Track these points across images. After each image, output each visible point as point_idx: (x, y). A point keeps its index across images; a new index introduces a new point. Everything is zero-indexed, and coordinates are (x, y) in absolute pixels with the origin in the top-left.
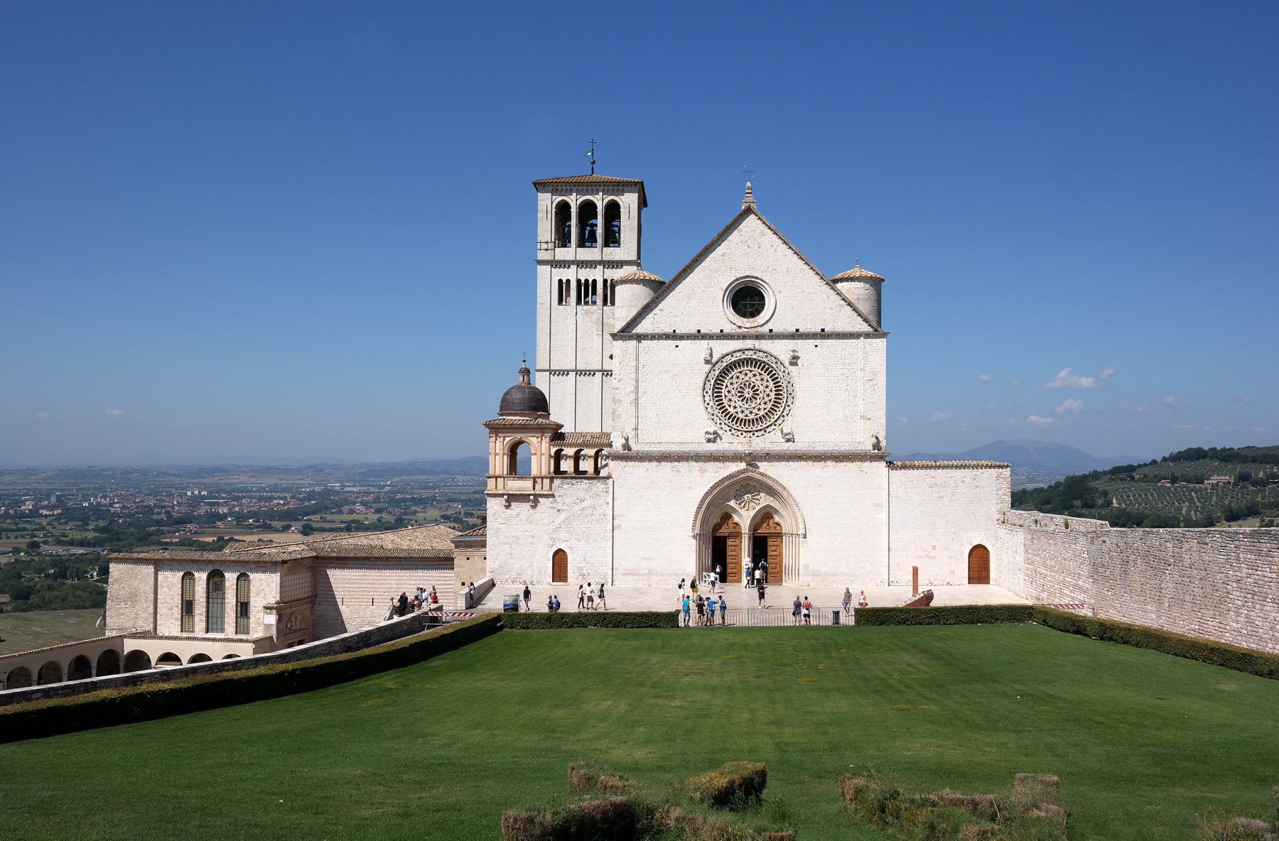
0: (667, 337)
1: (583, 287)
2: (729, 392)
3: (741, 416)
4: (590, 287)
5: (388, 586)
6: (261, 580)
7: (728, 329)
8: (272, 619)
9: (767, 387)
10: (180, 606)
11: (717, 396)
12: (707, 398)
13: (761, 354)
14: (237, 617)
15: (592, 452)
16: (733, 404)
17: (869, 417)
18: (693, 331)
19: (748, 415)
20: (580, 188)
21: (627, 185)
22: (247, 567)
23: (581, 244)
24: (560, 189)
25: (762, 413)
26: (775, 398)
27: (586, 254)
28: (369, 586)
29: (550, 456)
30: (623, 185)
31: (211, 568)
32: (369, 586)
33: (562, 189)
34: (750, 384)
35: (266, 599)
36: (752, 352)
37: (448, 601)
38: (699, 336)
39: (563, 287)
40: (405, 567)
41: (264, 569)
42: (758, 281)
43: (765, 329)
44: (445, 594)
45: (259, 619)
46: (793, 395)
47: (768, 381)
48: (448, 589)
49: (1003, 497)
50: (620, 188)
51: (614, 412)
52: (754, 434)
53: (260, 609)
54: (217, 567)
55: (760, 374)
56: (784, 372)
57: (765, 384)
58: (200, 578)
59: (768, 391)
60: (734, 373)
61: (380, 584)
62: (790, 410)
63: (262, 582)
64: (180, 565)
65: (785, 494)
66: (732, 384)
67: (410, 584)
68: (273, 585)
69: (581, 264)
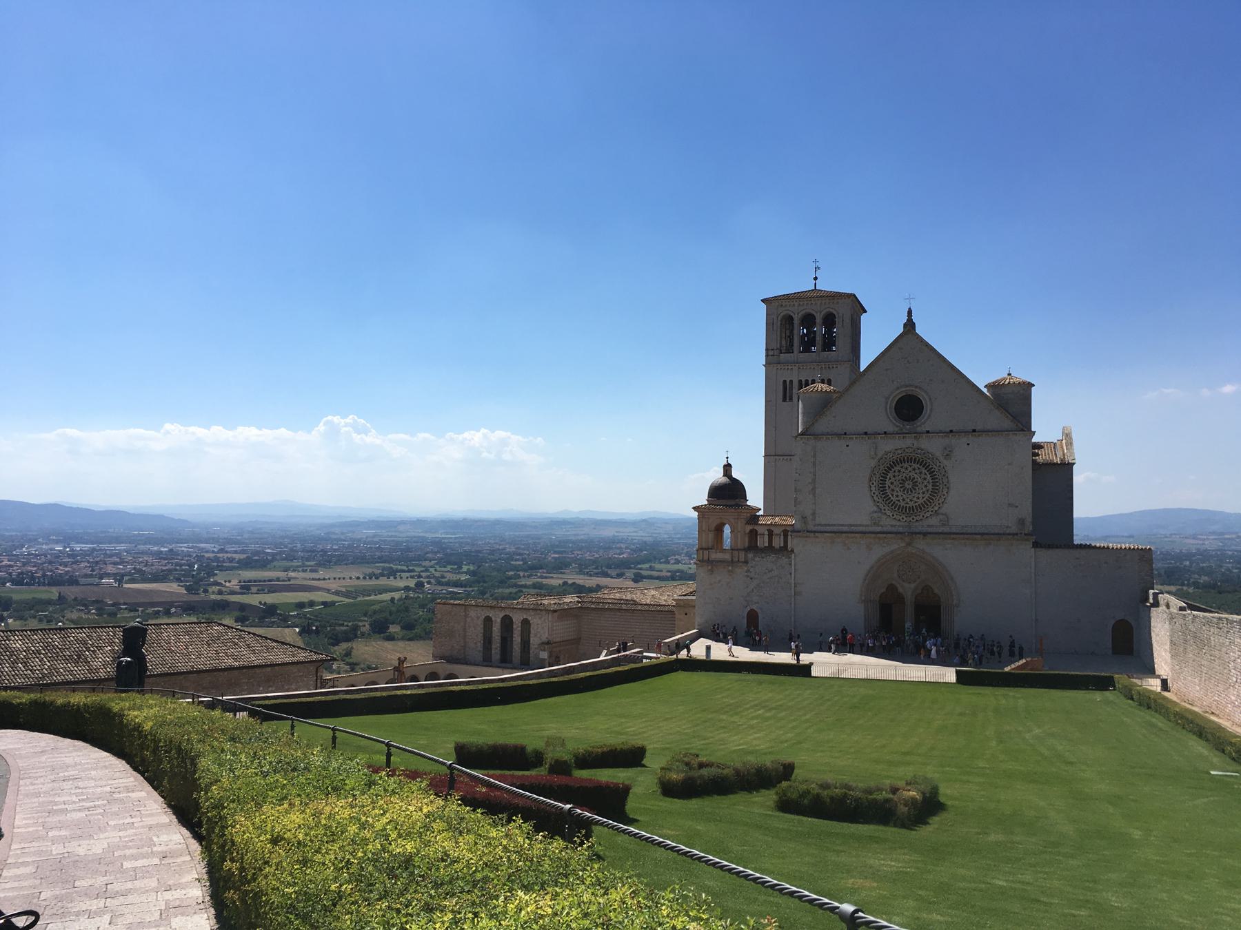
0: (838, 435)
2: (892, 483)
3: (902, 504)
7: (890, 429)
8: (544, 655)
9: (925, 479)
10: (482, 642)
11: (882, 488)
12: (873, 489)
13: (919, 451)
16: (895, 493)
17: (1017, 505)
19: (910, 503)
20: (801, 303)
24: (784, 304)
25: (921, 501)
26: (932, 489)
29: (745, 532)
30: (838, 299)
31: (502, 615)
32: (619, 632)
34: (910, 477)
42: (917, 390)
43: (925, 430)
46: (948, 485)
47: (925, 474)
49: (1146, 577)
50: (835, 301)
51: (796, 499)
52: (913, 519)
53: (536, 646)
54: (508, 614)
55: (919, 469)
56: (940, 466)
57: (923, 476)
58: (496, 620)
59: (926, 482)
62: (945, 499)
66: (894, 476)
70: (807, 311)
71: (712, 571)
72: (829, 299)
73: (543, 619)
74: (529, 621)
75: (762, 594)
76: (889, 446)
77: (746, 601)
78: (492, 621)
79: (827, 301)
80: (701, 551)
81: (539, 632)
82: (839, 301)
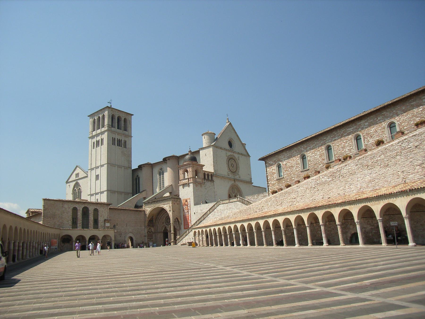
1: (118, 141)
5: (121, 219)
7: (229, 149)
10: (71, 220)
22: (97, 206)
23: (118, 128)
24: (113, 111)
25: (235, 170)
27: (119, 131)
31: (83, 206)
35: (104, 218)
38: (225, 149)
39: (114, 140)
40: (126, 213)
41: (103, 207)
44: (136, 223)
45: (102, 225)
50: (128, 115)
54: (86, 205)
58: (80, 210)
60: (230, 160)
64: (71, 204)
65: (240, 190)
67: (127, 219)
68: (107, 213)
69: (119, 134)
70: (120, 115)
71: (196, 186)
73: (105, 209)
74: (98, 209)
76: (229, 153)
78: (77, 210)
80: (193, 178)
81: (103, 214)
82: (129, 115)
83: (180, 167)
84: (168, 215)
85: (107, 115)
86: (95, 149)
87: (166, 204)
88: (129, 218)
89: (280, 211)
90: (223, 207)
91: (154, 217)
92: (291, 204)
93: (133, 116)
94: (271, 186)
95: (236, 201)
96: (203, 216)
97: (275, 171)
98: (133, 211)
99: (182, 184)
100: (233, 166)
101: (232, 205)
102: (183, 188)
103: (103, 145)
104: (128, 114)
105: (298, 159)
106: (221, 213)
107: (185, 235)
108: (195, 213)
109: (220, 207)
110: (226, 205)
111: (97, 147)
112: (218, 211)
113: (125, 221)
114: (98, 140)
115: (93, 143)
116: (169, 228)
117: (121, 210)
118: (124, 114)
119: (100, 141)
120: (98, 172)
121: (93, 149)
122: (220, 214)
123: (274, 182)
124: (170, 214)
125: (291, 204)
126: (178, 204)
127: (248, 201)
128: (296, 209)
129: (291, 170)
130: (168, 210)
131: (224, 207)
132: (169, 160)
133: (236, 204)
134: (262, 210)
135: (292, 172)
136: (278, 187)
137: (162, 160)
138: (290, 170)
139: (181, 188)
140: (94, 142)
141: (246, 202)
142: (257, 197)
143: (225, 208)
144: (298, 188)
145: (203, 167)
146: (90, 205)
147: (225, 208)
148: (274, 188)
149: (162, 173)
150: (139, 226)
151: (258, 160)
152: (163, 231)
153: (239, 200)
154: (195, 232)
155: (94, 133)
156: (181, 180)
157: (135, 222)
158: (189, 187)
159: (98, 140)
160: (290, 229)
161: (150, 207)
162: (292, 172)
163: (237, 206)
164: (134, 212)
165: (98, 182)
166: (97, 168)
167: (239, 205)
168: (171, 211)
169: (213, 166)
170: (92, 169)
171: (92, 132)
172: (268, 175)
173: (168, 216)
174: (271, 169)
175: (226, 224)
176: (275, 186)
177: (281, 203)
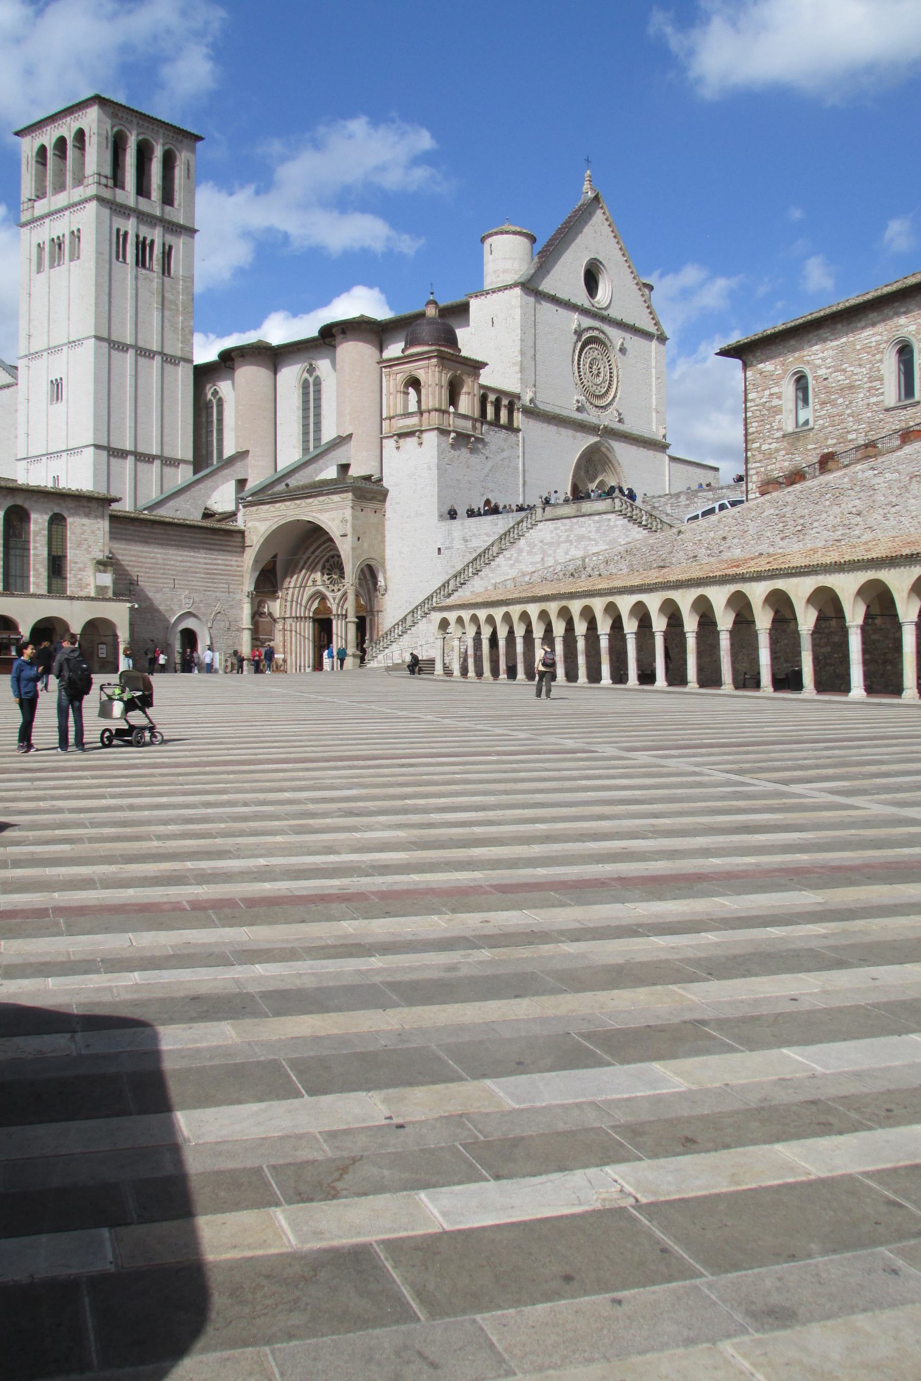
1: (140, 246)
4: (148, 248)
5: (153, 561)
6: (83, 525)
7: (587, 305)
14: (49, 577)
15: (505, 402)
18: (567, 299)
20: (141, 123)
21: (187, 138)
22: (64, 505)
24: (120, 115)
25: (603, 390)
28: (133, 559)
30: (183, 136)
31: (9, 502)
32: (133, 559)
33: (122, 117)
35: (89, 553)
36: (597, 332)
37: (215, 585)
39: (121, 238)
41: (87, 510)
43: (605, 313)
44: (212, 576)
45: (81, 579)
48: (215, 569)
50: (180, 138)
53: (81, 566)
54: (19, 501)
61: (145, 557)
63: (85, 528)
72: (174, 132)
75: (496, 480)
77: (483, 487)
79: (171, 135)
81: (86, 540)
82: (184, 139)
83: (390, 366)
84: (332, 553)
85: (95, 130)
86: (43, 276)
87: (332, 509)
88: (185, 559)
89: (799, 561)
90: (551, 532)
91: (279, 557)
92: (839, 533)
93: (199, 145)
94: (760, 461)
95: (605, 513)
96: (475, 559)
97: (780, 402)
98: (198, 531)
99: (395, 435)
100: (596, 372)
101: (590, 525)
102: (398, 448)
103: (78, 258)
104: (179, 134)
105: (881, 361)
106: (544, 552)
107: (400, 633)
108: (439, 549)
109: (541, 530)
110: (564, 525)
111: (52, 266)
112: (532, 545)
113: (169, 570)
114: (58, 238)
115: (35, 250)
116: (337, 601)
117: (156, 526)
118: (164, 134)
119: (67, 242)
120: (57, 367)
121: (39, 272)
122: (540, 560)
123: (774, 446)
124: (345, 548)
125: (842, 535)
126: (375, 512)
127: (651, 515)
128: (864, 553)
129: (847, 403)
130: (338, 534)
131: (557, 534)
132: (344, 332)
133: (606, 523)
134: (720, 552)
135: (849, 411)
136: (786, 464)
137: (315, 334)
138: (840, 401)
139: (389, 444)
140: (39, 245)
141: (644, 518)
142: (688, 502)
143: (560, 537)
144: (876, 472)
145: (481, 371)
146: (36, 502)
147: (560, 537)
148: (769, 468)
149: (314, 385)
150: (223, 592)
151: (717, 354)
152: (311, 615)
153: (616, 509)
154: (444, 624)
155: (41, 207)
156: (390, 418)
157: (208, 574)
158: (421, 444)
159: (58, 238)
160: (826, 631)
161: (266, 519)
162: (849, 411)
163: (607, 533)
164: (204, 536)
165: (60, 407)
166: (52, 350)
167: (616, 526)
168: (349, 538)
169: (517, 368)
170: (33, 356)
171: (35, 201)
172: (749, 414)
173: (333, 557)
174: (767, 392)
175: (572, 596)
176: (774, 460)
177: (799, 528)
